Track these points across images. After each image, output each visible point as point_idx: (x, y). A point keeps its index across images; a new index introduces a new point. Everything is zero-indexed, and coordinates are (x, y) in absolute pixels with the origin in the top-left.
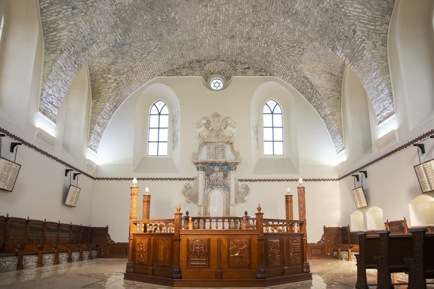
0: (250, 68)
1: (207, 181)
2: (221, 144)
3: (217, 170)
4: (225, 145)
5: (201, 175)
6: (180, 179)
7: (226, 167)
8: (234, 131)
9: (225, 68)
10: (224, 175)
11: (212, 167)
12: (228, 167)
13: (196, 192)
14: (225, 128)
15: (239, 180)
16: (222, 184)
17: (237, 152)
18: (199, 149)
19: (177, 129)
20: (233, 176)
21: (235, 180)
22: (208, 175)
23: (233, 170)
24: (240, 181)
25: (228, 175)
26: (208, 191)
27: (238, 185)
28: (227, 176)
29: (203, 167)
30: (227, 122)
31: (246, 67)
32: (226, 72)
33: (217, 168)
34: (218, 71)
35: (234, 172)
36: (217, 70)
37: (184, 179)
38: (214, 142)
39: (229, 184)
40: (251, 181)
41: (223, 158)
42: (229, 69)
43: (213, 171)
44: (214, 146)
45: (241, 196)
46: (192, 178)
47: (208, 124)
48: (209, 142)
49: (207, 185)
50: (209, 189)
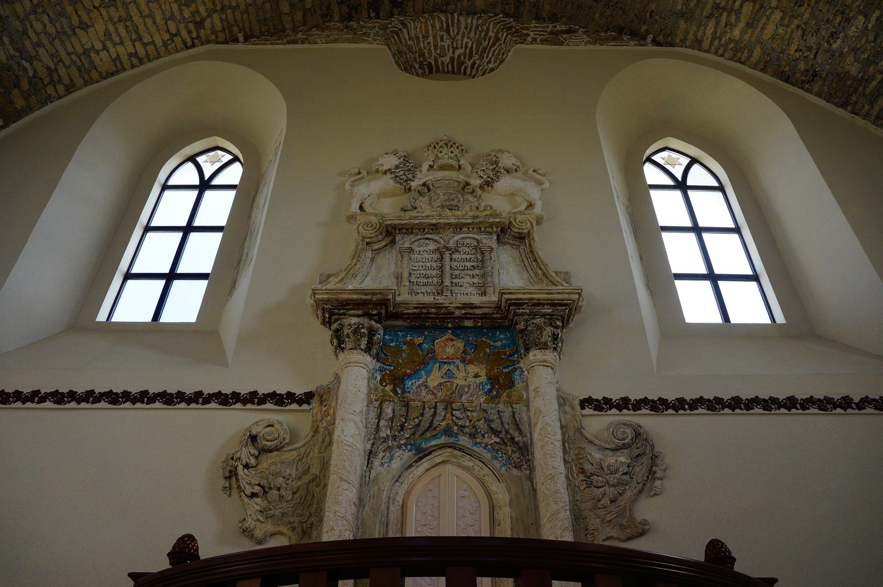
0: (576, 32)
1: (388, 410)
2: (468, 237)
3: (450, 350)
4: (489, 241)
5: (357, 377)
6: (225, 399)
7: (500, 341)
8: (534, 193)
9: (479, 44)
10: (493, 380)
11: (419, 340)
12: (512, 331)
13: (315, 470)
14: (488, 184)
15: (586, 402)
16: (481, 424)
17: (556, 273)
18: (356, 256)
19: (262, 202)
20: (546, 384)
21: (563, 400)
22: (397, 380)
23: (544, 347)
24: (588, 411)
25: (516, 376)
26: (396, 464)
27: (579, 430)
28: (511, 384)
29: (372, 332)
30: (496, 163)
31: (558, 28)
32: (481, 57)
33: (449, 346)
34: (452, 59)
35: (549, 356)
36: (450, 54)
37: (253, 398)
38: (435, 228)
39: (525, 427)
40: (658, 406)
41: (484, 294)
42: (497, 39)
43: (424, 361)
44: (432, 246)
45: (611, 491)
46: (299, 391)
47: (404, 171)
48: (409, 230)
49: (385, 432)
50: (402, 457)
